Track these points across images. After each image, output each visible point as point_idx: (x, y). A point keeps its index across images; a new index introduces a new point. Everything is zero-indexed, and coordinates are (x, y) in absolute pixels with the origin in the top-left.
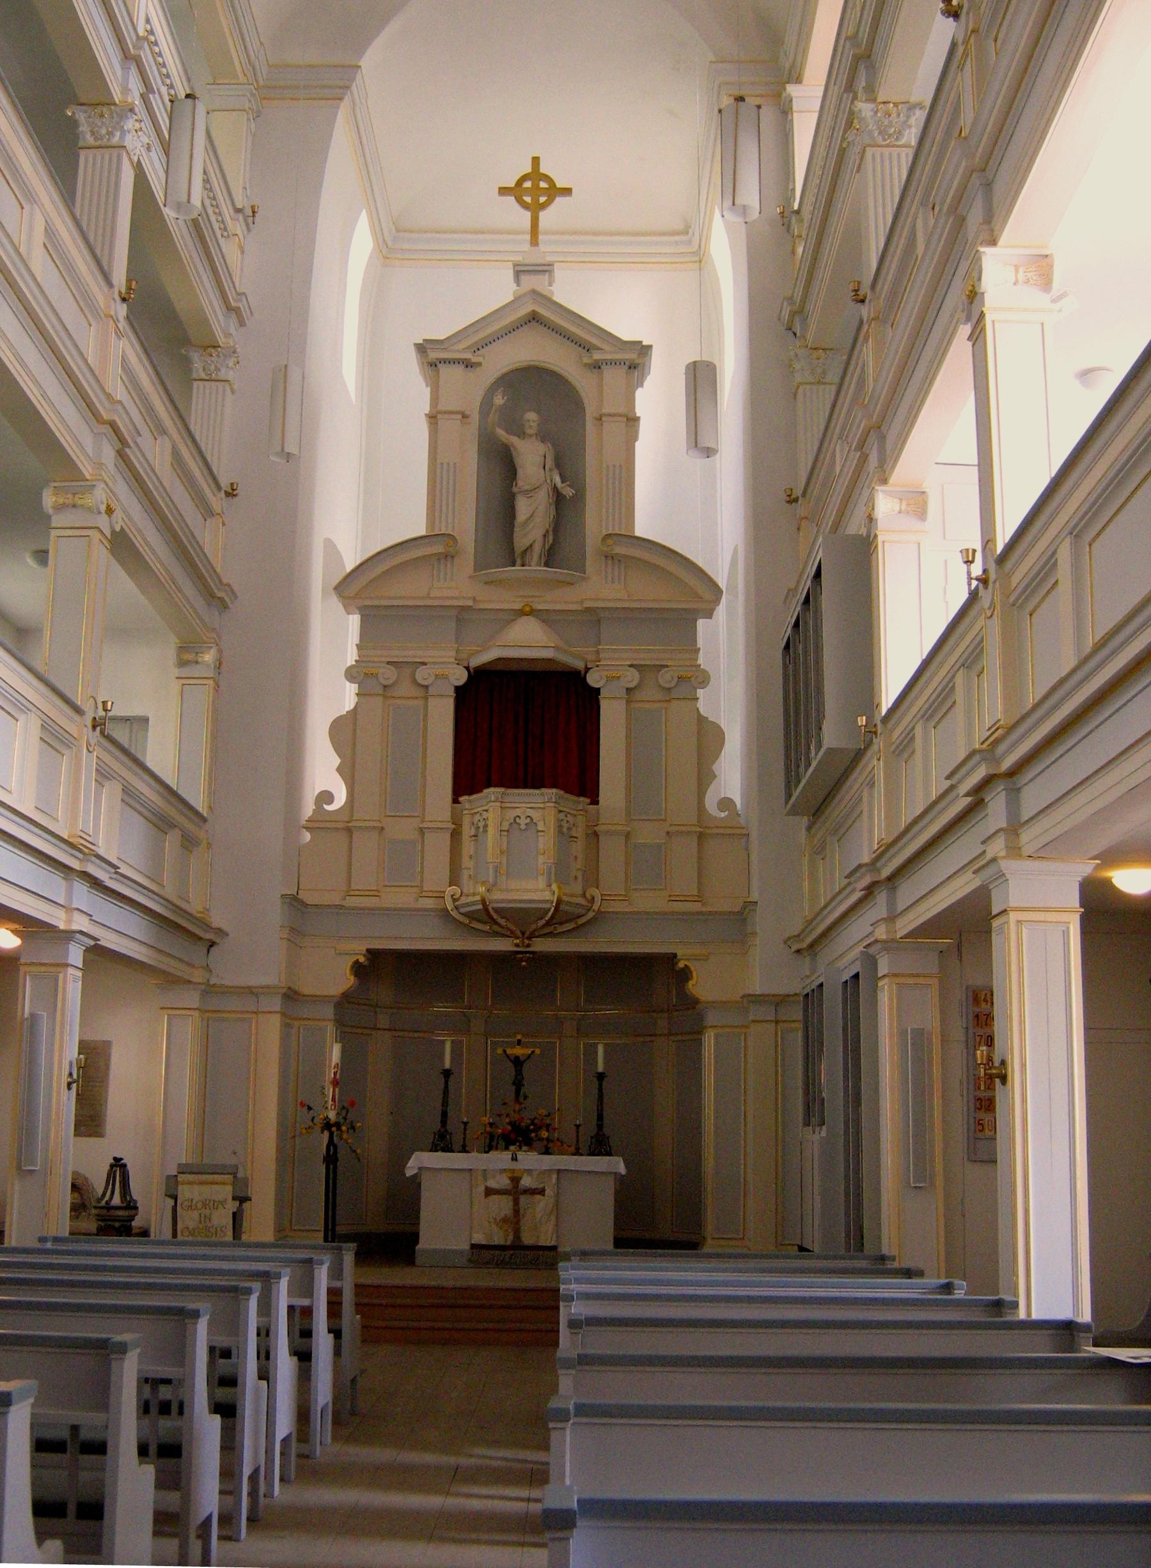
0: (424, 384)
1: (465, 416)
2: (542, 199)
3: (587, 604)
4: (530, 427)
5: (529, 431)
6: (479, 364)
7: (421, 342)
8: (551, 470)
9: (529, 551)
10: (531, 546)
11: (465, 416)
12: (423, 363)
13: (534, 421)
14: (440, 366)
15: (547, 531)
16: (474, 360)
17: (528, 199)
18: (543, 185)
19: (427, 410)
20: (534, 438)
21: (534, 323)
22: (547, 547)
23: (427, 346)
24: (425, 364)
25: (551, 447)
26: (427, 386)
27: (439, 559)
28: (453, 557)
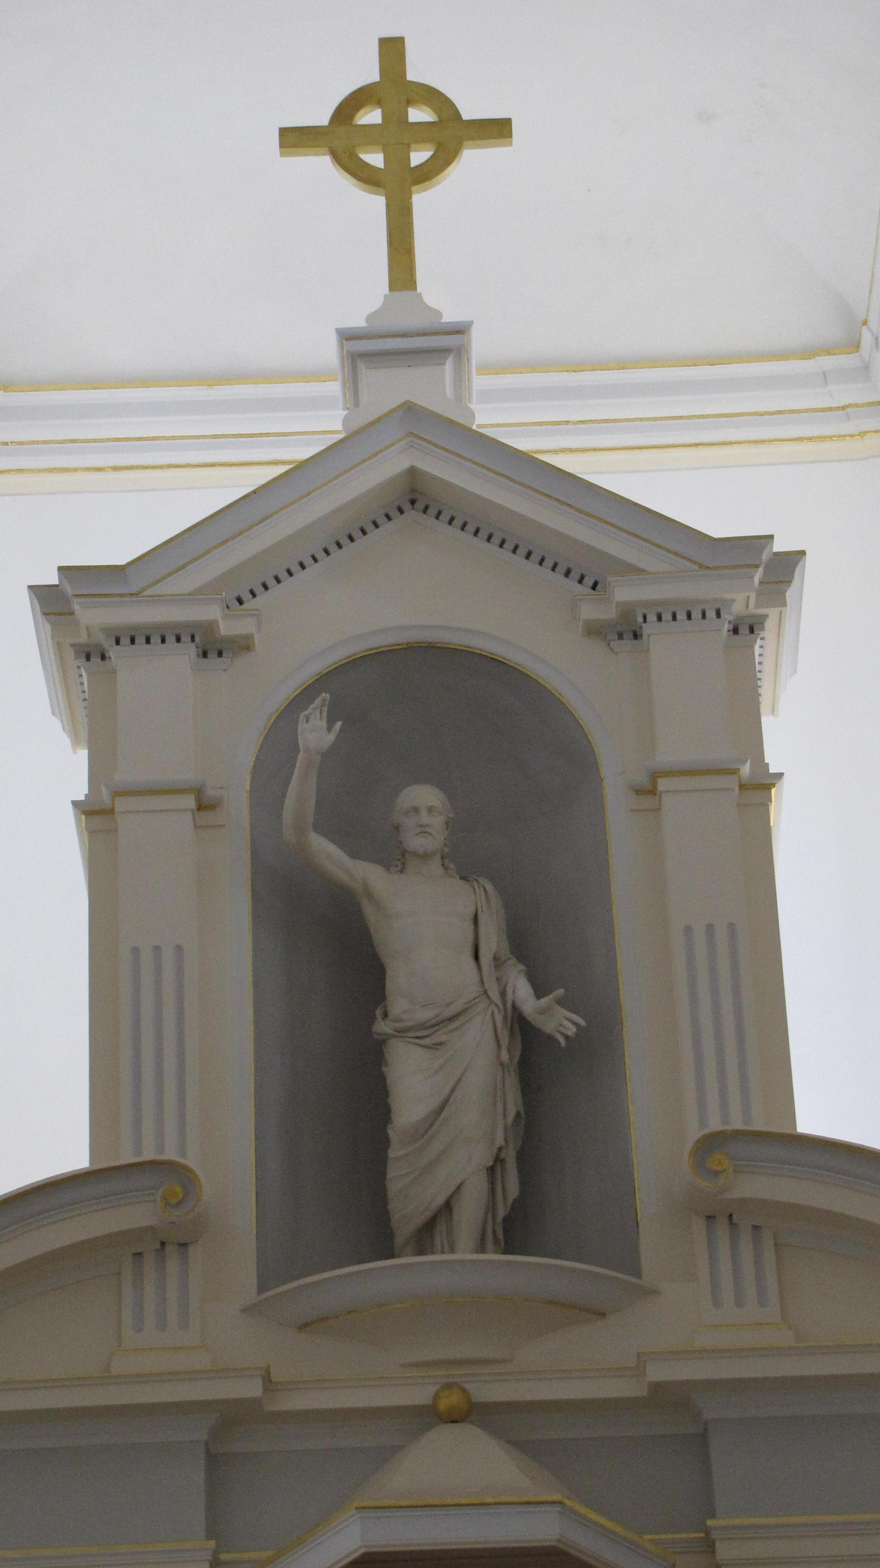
0: (65, 740)
1: (205, 805)
2: (418, 157)
3: (658, 1373)
4: (423, 830)
5: (416, 843)
6: (244, 645)
7: (53, 579)
8: (498, 962)
9: (441, 1228)
10: (448, 1206)
11: (205, 805)
12: (59, 647)
13: (430, 810)
14: (113, 652)
15: (499, 1160)
16: (226, 628)
17: (375, 159)
18: (418, 115)
19: (81, 791)
20: (435, 865)
21: (411, 514)
22: (501, 1212)
23: (69, 589)
24: (70, 654)
25: (489, 887)
26: (76, 741)
27: (139, 1255)
28: (183, 1245)
